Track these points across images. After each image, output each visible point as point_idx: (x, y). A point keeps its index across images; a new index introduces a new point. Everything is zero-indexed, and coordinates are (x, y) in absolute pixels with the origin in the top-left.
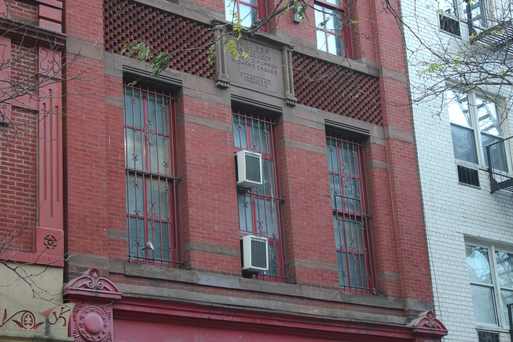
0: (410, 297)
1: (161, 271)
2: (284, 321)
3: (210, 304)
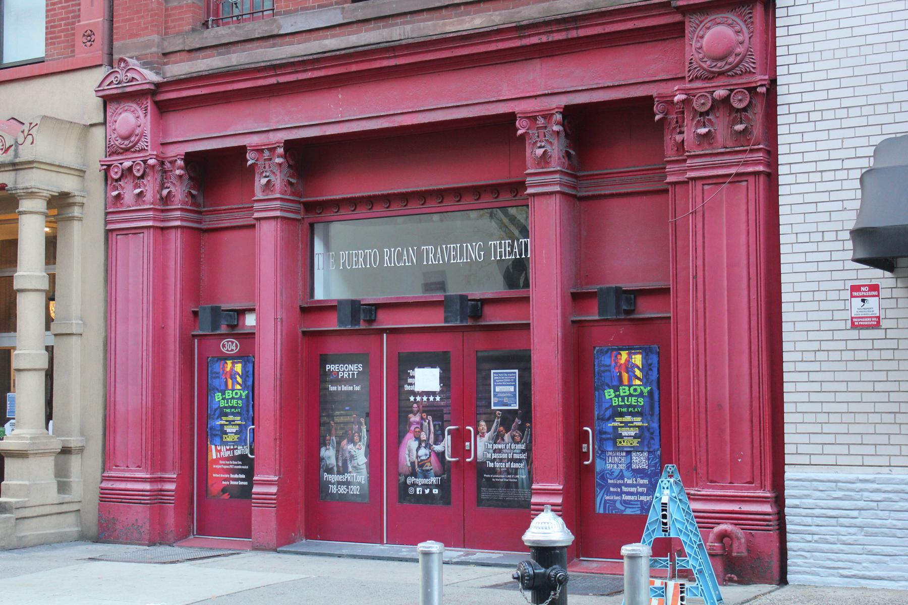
1: (229, 31)
2: (395, 57)
3: (268, 64)
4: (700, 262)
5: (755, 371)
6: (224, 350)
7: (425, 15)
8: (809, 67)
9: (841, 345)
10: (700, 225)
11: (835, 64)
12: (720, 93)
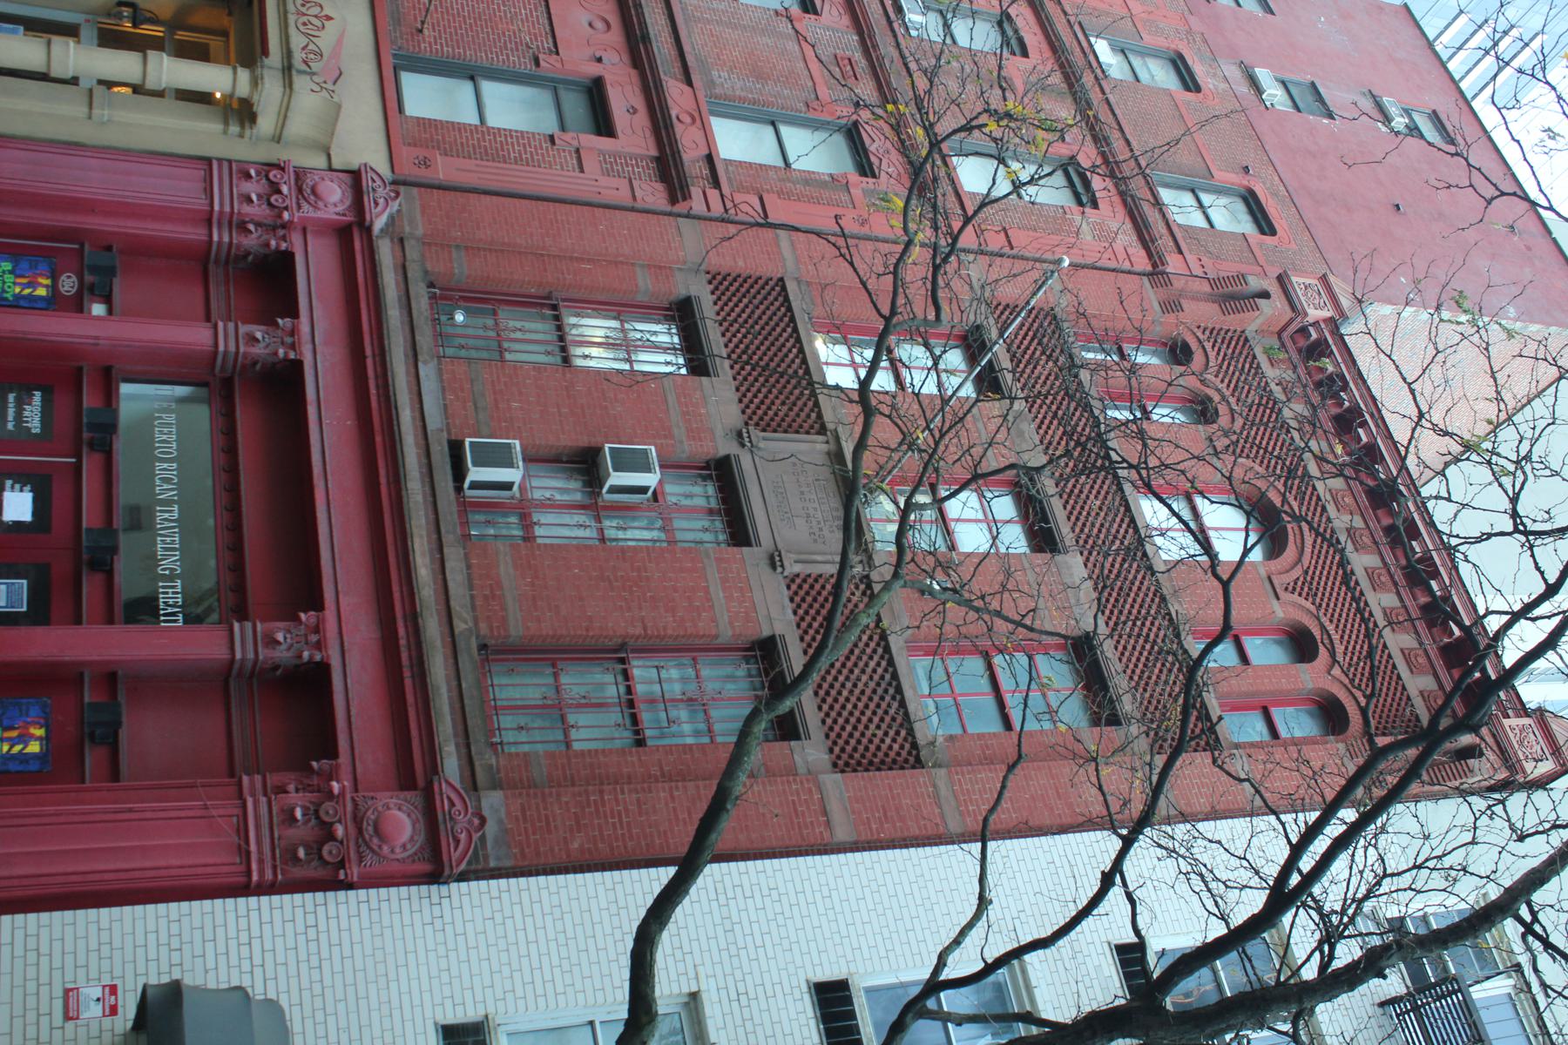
0: (506, 797)
4: (148, 815)
5: (16, 882)
6: (63, 277)
7: (432, 517)
8: (366, 924)
9: (44, 978)
10: (191, 813)
11: (368, 951)
12: (340, 831)
